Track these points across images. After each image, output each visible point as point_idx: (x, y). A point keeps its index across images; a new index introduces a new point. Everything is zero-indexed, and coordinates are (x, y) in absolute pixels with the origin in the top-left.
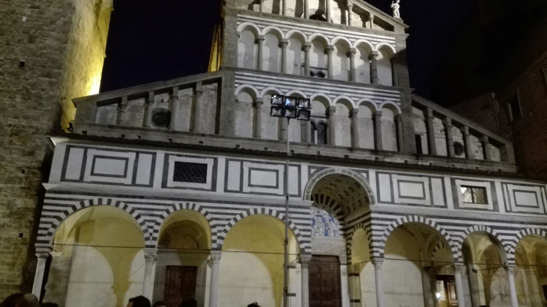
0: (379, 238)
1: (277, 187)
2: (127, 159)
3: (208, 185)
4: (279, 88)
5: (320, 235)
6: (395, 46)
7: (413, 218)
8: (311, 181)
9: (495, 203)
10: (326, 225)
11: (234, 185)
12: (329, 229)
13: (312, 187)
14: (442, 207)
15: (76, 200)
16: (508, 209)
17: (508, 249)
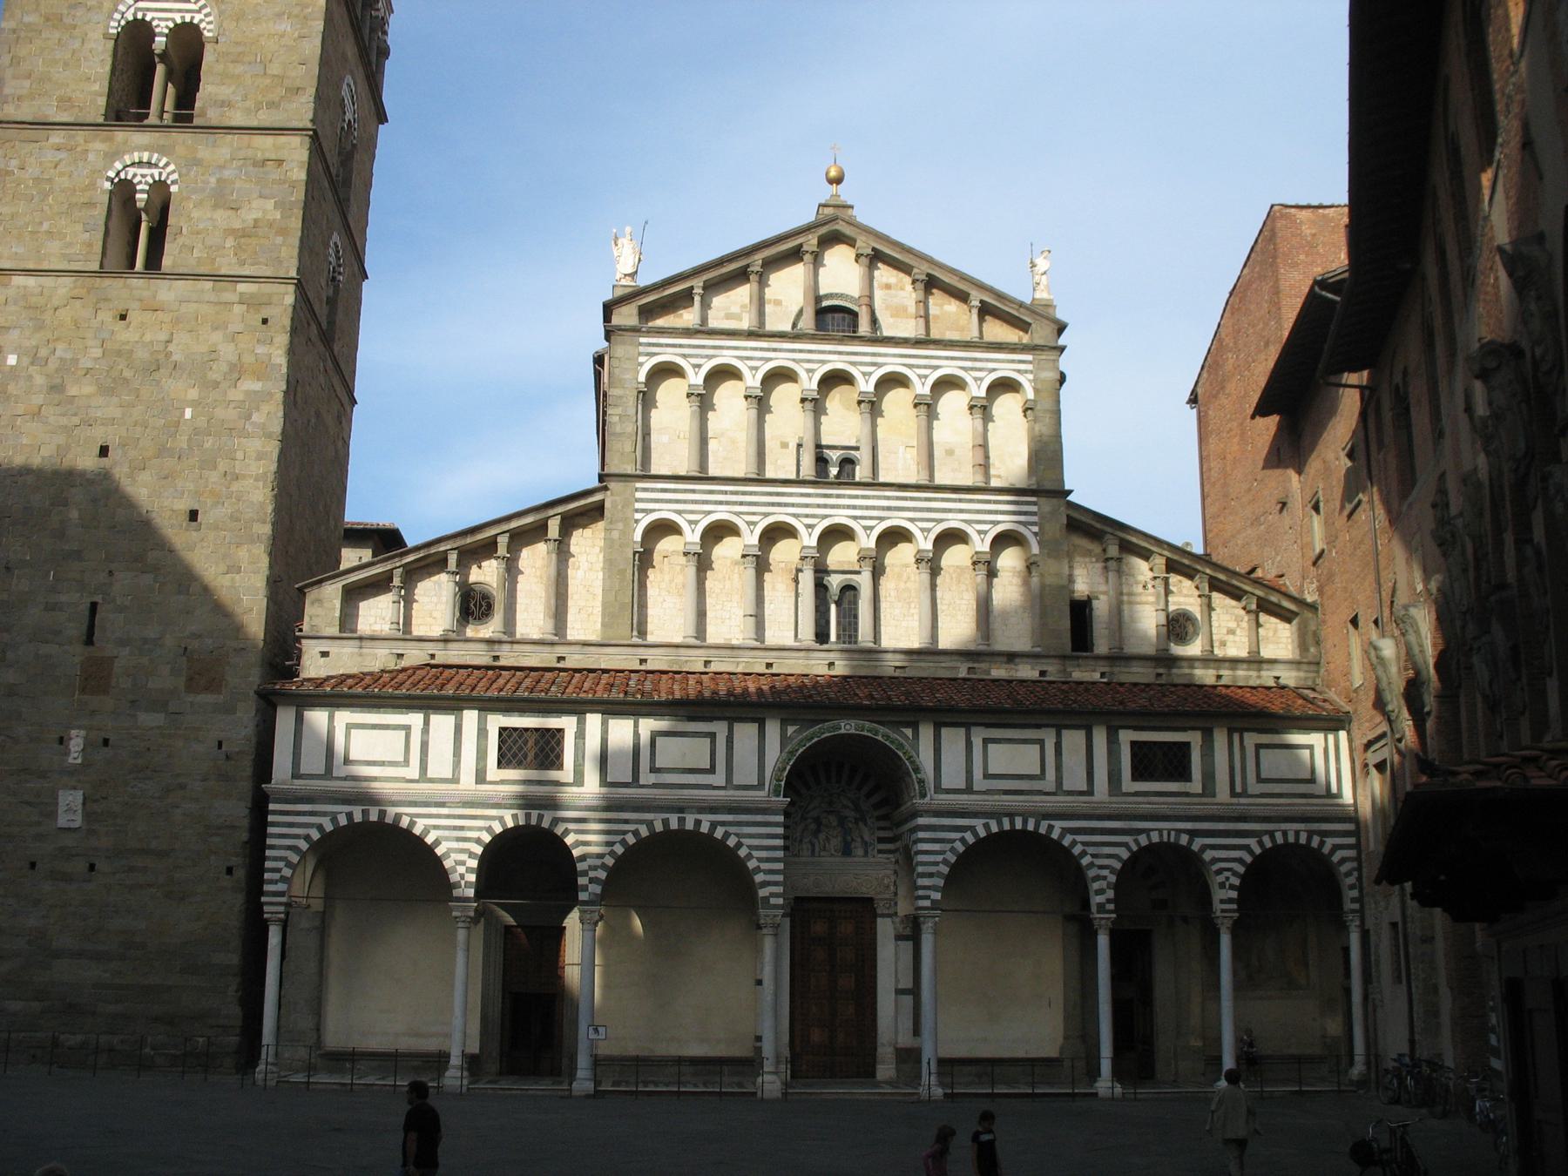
0: (932, 869)
1: (712, 770)
2: (407, 728)
6: (1031, 377)
7: (1012, 823)
8: (784, 755)
9: (1209, 777)
13: (788, 767)
14: (1081, 793)
15: (324, 814)
16: (1238, 789)
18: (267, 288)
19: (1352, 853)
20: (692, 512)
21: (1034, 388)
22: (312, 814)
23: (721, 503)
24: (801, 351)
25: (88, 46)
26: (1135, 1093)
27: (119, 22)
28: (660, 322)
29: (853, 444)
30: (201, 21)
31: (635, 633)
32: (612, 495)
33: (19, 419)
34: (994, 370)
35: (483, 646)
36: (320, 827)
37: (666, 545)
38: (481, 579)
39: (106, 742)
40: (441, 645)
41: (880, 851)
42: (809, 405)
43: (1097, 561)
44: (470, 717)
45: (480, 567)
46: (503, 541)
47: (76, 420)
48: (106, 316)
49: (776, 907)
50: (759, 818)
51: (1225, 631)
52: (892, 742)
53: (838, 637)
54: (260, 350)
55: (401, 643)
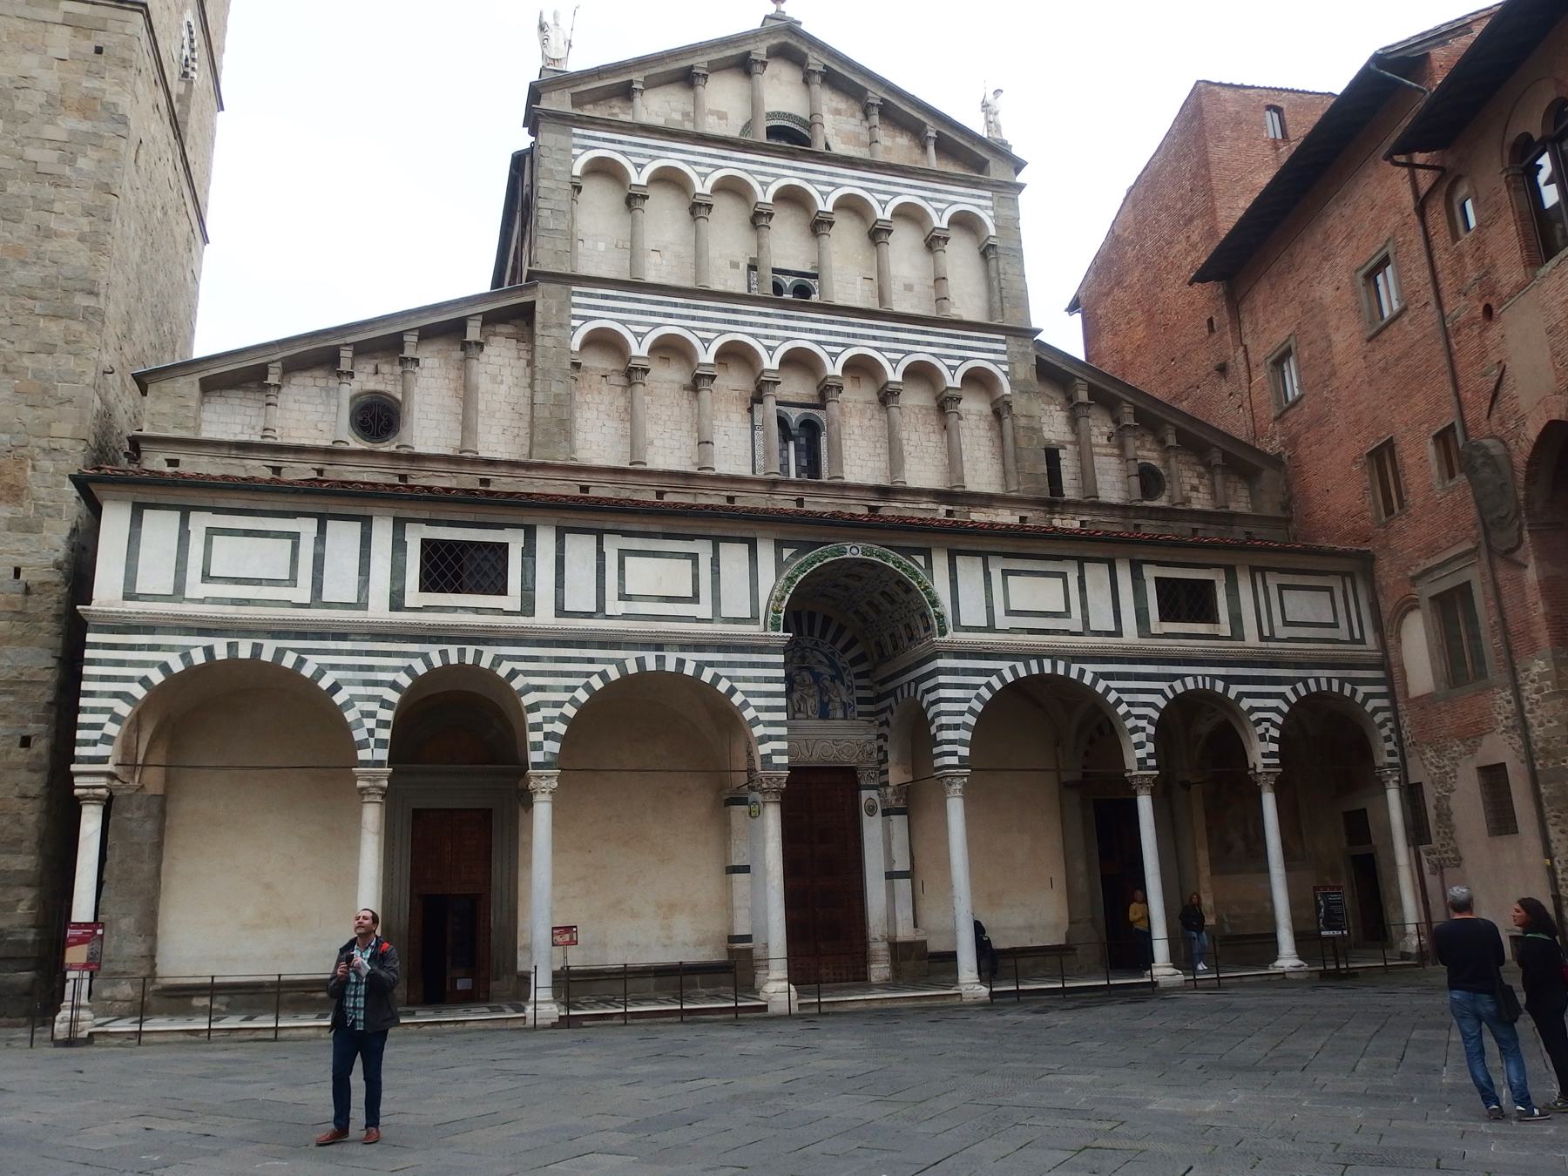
0: (958, 720)
1: (695, 598)
2: (295, 537)
3: (512, 600)
5: (808, 718)
6: (991, 213)
7: (1041, 666)
8: (782, 581)
9: (1236, 619)
10: (823, 691)
11: (580, 595)
12: (830, 700)
13: (788, 597)
14: (1109, 634)
15: (171, 648)
16: (1266, 633)
17: (1263, 731)
19: (1385, 703)
20: (638, 323)
21: (996, 225)
26: (1218, 978)
29: (807, 269)
34: (955, 203)
36: (164, 667)
41: (860, 714)
43: (1062, 410)
49: (778, 767)
50: (755, 658)
51: (1188, 488)
52: (904, 570)
54: (89, 83)
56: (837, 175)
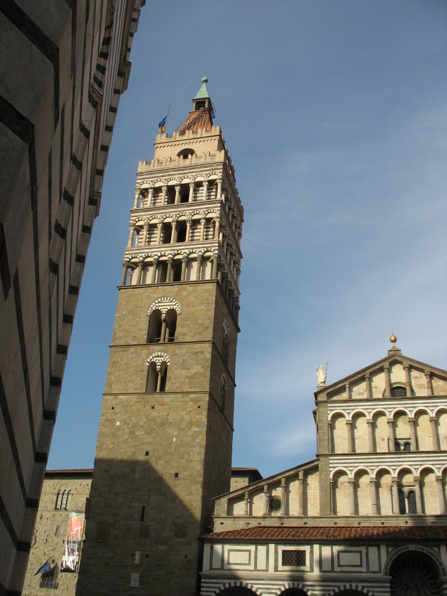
1: (361, 566)
2: (249, 551)
4: (367, 466)
8: (388, 559)
13: (390, 564)
15: (221, 583)
18: (199, 395)
20: (350, 467)
22: (217, 583)
23: (361, 463)
24: (386, 405)
25: (141, 319)
27: (151, 311)
28: (335, 398)
29: (408, 437)
30: (176, 308)
31: (332, 513)
32: (321, 462)
33: (120, 443)
35: (277, 519)
36: (219, 588)
37: (342, 479)
38: (276, 494)
39: (147, 556)
40: (262, 519)
42: (391, 424)
44: (272, 546)
45: (276, 490)
46: (283, 481)
47: (138, 443)
48: (148, 408)
50: (380, 585)
53: (409, 511)
54: (198, 417)
55: (248, 519)
56: (415, 403)
